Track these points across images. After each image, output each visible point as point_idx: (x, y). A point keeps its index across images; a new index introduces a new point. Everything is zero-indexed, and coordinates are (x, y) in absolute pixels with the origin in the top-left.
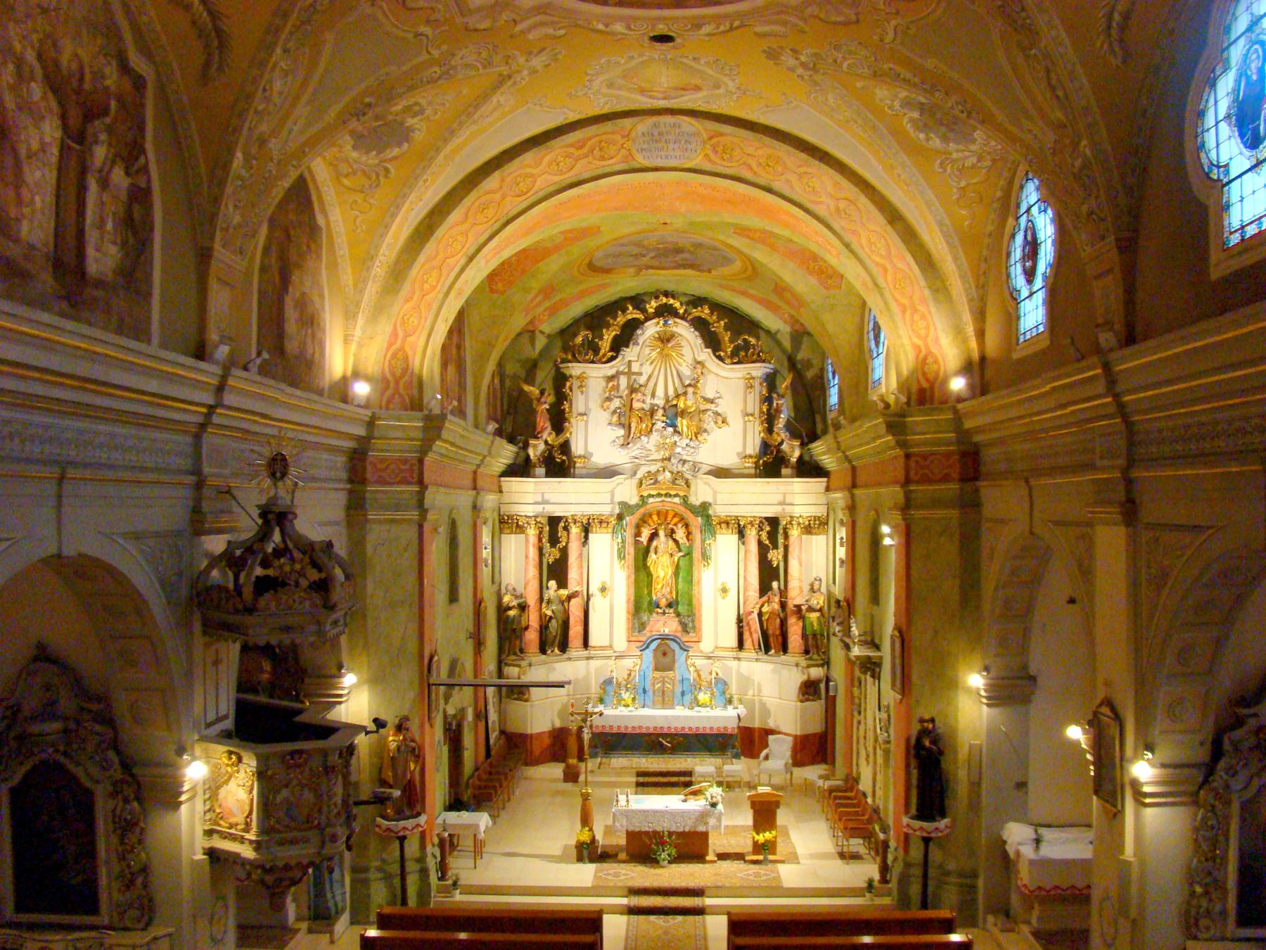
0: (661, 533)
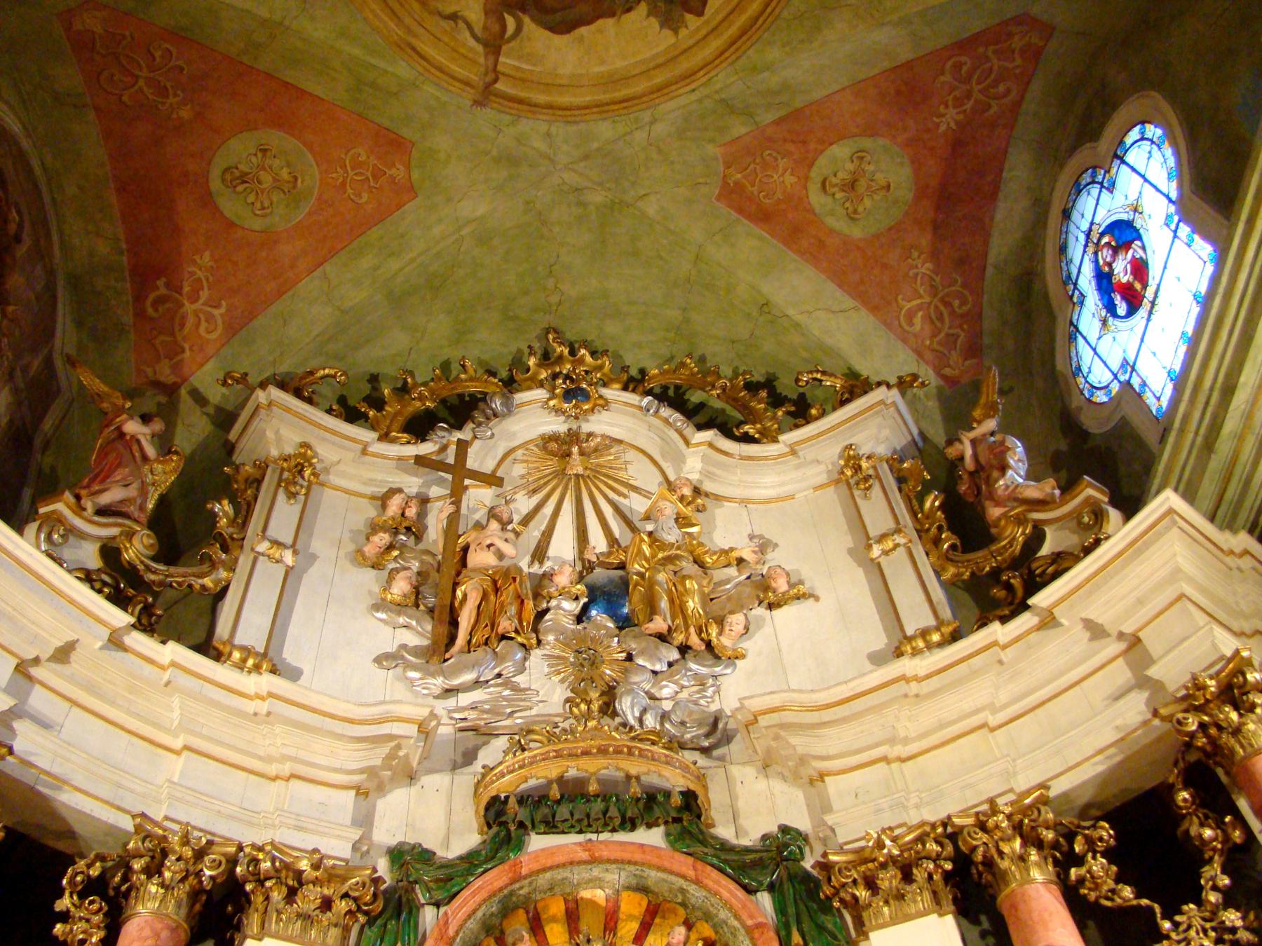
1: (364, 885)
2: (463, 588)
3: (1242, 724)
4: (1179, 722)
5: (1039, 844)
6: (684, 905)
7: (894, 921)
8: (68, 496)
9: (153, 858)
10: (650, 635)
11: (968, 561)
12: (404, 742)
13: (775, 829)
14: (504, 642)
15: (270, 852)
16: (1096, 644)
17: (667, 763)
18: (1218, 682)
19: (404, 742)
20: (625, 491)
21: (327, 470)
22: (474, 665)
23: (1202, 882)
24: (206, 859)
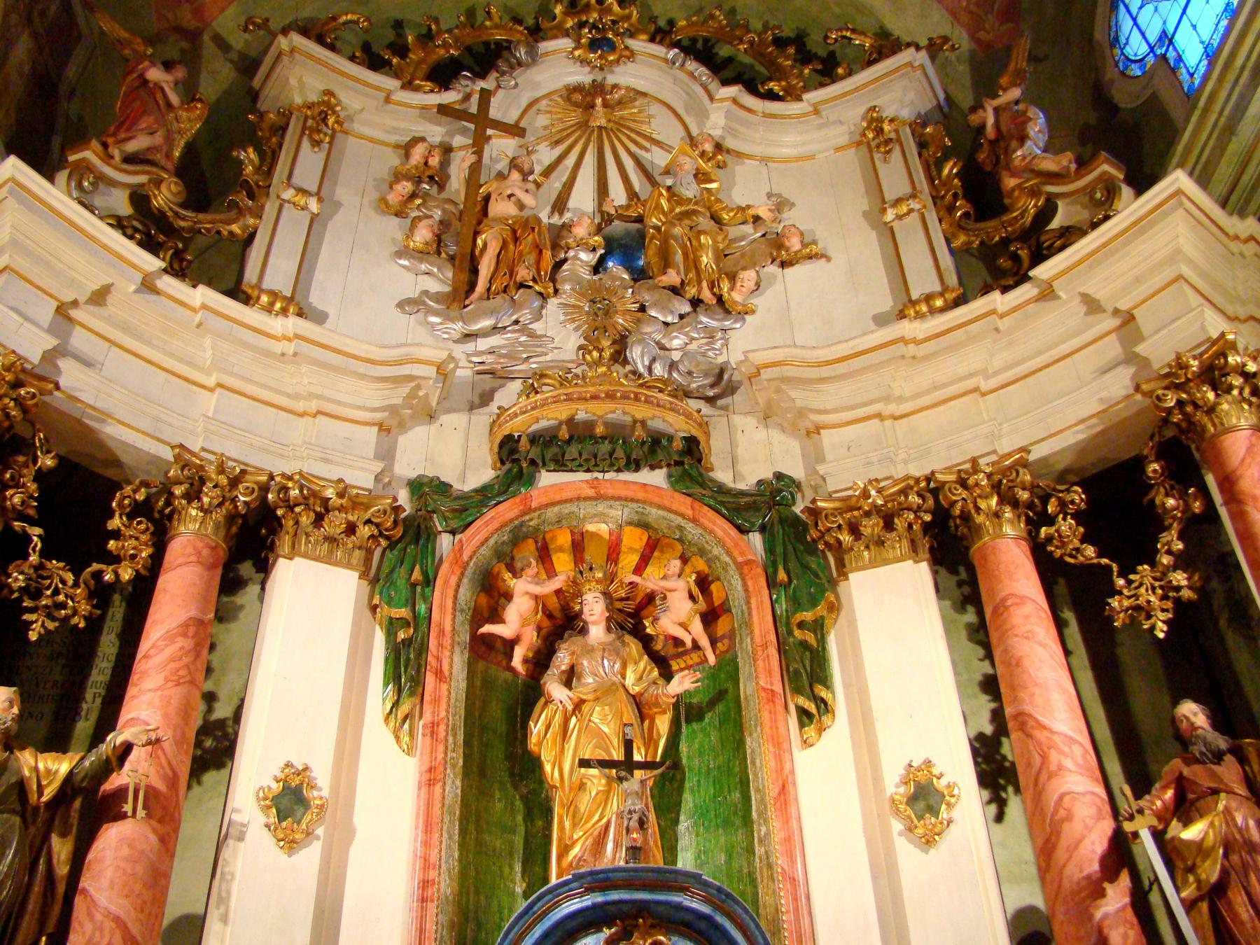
0: (594, 608)
1: (385, 512)
2: (484, 236)
3: (1216, 404)
4: (1158, 398)
5: (1015, 504)
6: (680, 540)
7: (873, 564)
8: (95, 144)
9: (192, 484)
10: (664, 288)
11: (980, 230)
12: (423, 383)
13: (770, 476)
14: (521, 291)
15: (298, 481)
16: (1091, 318)
17: (672, 410)
18: (1201, 362)
19: (423, 383)
20: (647, 144)
21: (350, 118)
22: (492, 313)
23: (1159, 546)
24: (240, 486)
